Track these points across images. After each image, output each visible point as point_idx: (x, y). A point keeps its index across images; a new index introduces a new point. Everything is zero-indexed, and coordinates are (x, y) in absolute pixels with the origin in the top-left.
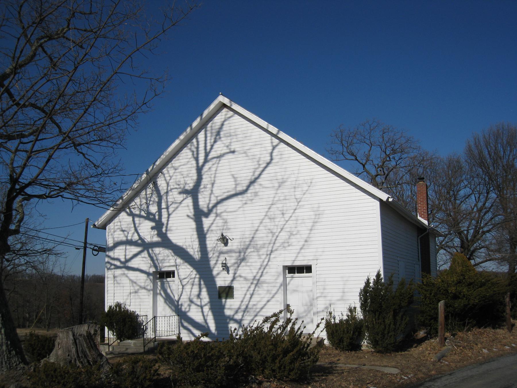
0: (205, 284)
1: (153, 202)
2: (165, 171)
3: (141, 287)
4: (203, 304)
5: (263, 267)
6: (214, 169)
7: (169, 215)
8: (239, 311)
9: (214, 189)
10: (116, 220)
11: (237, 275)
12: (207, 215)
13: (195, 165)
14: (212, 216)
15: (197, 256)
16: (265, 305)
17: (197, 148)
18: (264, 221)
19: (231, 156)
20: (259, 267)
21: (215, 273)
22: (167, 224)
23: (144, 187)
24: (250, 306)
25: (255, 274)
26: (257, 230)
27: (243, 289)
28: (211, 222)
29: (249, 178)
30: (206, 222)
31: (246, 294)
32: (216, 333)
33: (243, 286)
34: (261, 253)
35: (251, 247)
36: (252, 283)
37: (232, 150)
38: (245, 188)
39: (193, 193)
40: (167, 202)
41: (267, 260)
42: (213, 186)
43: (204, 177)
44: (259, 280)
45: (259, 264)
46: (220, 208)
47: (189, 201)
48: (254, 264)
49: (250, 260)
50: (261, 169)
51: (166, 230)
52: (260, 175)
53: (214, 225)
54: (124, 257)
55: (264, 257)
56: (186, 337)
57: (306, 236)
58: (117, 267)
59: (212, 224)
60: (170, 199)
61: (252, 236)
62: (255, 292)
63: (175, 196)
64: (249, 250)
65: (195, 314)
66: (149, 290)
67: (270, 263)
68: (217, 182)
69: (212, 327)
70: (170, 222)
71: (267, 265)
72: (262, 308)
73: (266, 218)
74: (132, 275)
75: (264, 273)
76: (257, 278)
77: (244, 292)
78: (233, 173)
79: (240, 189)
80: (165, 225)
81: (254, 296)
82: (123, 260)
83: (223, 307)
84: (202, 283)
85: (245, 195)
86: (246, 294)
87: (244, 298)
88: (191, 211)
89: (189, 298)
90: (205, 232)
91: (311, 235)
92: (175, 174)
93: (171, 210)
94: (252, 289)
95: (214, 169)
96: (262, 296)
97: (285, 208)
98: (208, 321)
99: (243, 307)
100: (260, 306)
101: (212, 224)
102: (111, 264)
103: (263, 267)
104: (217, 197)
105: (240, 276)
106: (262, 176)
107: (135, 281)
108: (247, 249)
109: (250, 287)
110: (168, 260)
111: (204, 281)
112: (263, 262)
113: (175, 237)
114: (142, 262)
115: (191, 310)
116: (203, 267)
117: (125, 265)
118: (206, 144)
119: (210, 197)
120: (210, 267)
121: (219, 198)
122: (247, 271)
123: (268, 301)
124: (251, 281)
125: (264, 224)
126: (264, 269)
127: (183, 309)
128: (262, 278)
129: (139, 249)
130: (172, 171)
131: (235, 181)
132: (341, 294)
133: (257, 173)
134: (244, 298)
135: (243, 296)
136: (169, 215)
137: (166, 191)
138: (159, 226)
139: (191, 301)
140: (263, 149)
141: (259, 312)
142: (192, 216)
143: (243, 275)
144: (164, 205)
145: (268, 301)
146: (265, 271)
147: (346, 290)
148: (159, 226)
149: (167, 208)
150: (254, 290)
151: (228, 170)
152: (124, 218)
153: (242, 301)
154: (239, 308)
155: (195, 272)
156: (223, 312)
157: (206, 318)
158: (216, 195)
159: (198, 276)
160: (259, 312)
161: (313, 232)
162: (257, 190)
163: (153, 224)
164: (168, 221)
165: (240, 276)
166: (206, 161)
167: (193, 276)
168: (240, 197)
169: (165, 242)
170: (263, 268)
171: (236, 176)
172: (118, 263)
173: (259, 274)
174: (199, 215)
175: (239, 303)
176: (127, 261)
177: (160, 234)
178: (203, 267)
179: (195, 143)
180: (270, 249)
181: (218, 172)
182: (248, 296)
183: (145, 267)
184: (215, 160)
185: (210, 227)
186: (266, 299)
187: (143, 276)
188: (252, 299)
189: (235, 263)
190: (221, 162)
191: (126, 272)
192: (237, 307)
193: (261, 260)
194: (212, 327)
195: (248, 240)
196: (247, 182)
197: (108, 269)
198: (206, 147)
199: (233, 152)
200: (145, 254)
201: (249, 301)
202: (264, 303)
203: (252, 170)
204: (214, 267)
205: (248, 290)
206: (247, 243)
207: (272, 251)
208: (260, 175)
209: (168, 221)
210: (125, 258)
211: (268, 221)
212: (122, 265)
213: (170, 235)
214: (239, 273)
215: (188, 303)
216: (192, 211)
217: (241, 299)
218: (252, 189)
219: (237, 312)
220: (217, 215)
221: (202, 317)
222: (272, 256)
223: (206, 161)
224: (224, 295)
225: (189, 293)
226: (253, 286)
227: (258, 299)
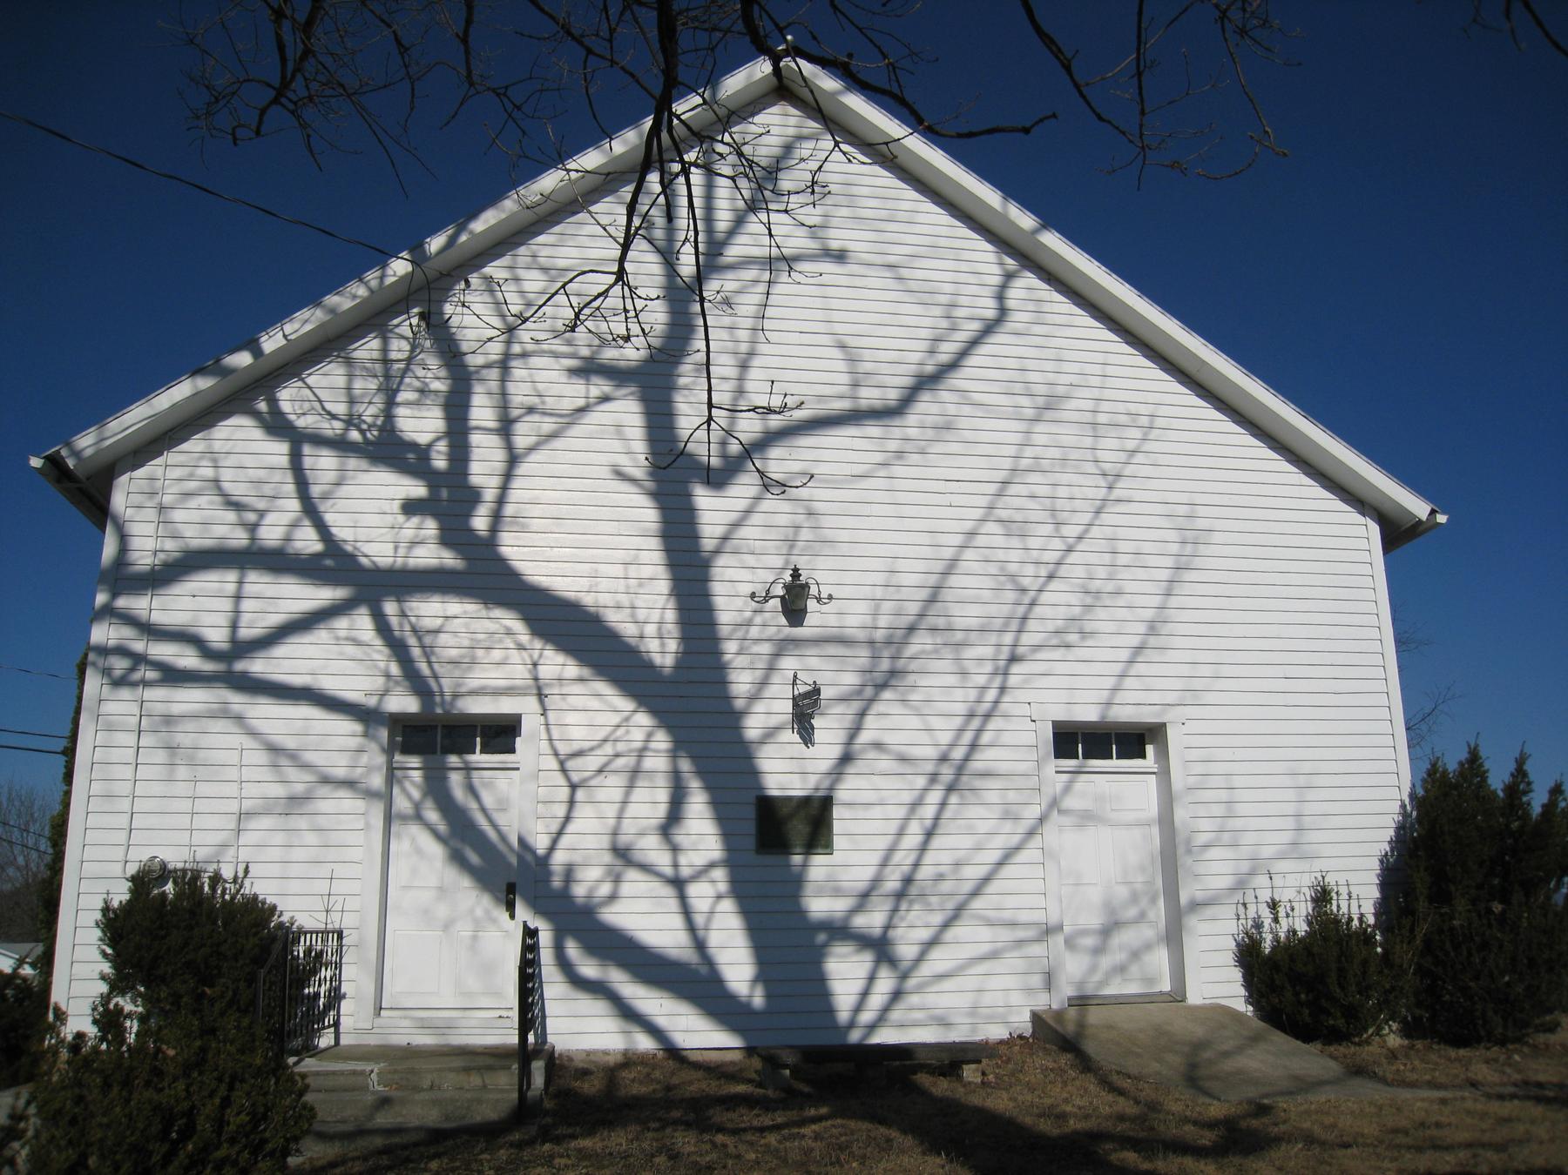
0: (701, 773)
1: (423, 391)
2: (495, 269)
3: (326, 780)
4: (691, 860)
5: (981, 716)
7: (513, 460)
10: (194, 445)
11: (865, 737)
12: (717, 479)
14: (744, 488)
15: (663, 650)
20: (961, 709)
21: (753, 726)
22: (504, 488)
23: (374, 319)
24: (925, 873)
25: (945, 738)
26: (955, 561)
28: (742, 504)
29: (916, 357)
30: (713, 510)
32: (758, 1001)
34: (970, 653)
36: (934, 777)
37: (834, 245)
38: (893, 395)
39: (654, 380)
40: (504, 394)
46: (779, 462)
47: (627, 412)
49: (924, 681)
50: (963, 336)
51: (497, 517)
52: (964, 353)
53: (756, 519)
54: (223, 620)
56: (581, 1028)
57: (1156, 601)
58: (173, 676)
59: (748, 512)
60: (520, 393)
61: (932, 580)
62: (948, 813)
63: (545, 380)
65: (645, 915)
66: (370, 794)
68: (763, 348)
69: (738, 968)
70: (516, 483)
74: (269, 715)
75: (986, 738)
76: (958, 753)
78: (839, 328)
79: (870, 396)
80: (490, 495)
82: (217, 636)
83: (795, 883)
84: (685, 765)
85: (897, 421)
87: (901, 833)
88: (635, 453)
89: (615, 833)
90: (708, 544)
91: (1173, 602)
93: (523, 435)
94: (935, 797)
96: (983, 827)
97: (1062, 492)
98: (714, 939)
100: (973, 873)
101: (748, 512)
102: (139, 659)
103: (981, 716)
106: (972, 360)
107: (290, 743)
108: (912, 629)
110: (485, 656)
111: (694, 758)
113: (531, 554)
114: (345, 658)
115: (626, 889)
116: (691, 700)
117: (231, 667)
120: (727, 698)
122: (913, 725)
124: (930, 767)
125: (980, 540)
126: (988, 716)
127: (579, 891)
129: (324, 595)
130: (534, 283)
131: (852, 360)
132: (1290, 823)
133: (947, 350)
134: (901, 833)
135: (893, 827)
136: (513, 460)
137: (496, 349)
138: (448, 499)
139: (623, 855)
140: (964, 267)
142: (639, 473)
143: (888, 738)
144: (482, 411)
146: (994, 724)
147: (1308, 809)
148: (448, 499)
149: (505, 427)
150: (943, 804)
151: (820, 315)
152: (241, 445)
153: (891, 850)
154: (876, 882)
155: (644, 719)
157: (701, 933)
159: (662, 741)
161: (1177, 589)
162: (952, 409)
163: (418, 490)
164: (508, 476)
167: (638, 735)
168: (873, 430)
169: (485, 575)
171: (850, 341)
172: (187, 659)
174: (673, 475)
175: (876, 858)
176: (242, 648)
177: (455, 533)
178: (691, 700)
180: (1008, 638)
181: (769, 312)
182: (915, 828)
183: (356, 685)
185: (736, 525)
187: (345, 729)
188: (936, 842)
191: (237, 701)
192: (868, 873)
194: (738, 968)
197: (119, 683)
199: (840, 256)
200: (362, 622)
204: (754, 698)
205: (916, 805)
208: (964, 353)
209: (508, 476)
210: (234, 626)
212: (209, 666)
213: (516, 549)
215: (607, 858)
216: (640, 447)
217: (884, 843)
218: (927, 407)
220: (767, 484)
221: (678, 921)
222: (1016, 668)
224: (798, 829)
225: (611, 811)
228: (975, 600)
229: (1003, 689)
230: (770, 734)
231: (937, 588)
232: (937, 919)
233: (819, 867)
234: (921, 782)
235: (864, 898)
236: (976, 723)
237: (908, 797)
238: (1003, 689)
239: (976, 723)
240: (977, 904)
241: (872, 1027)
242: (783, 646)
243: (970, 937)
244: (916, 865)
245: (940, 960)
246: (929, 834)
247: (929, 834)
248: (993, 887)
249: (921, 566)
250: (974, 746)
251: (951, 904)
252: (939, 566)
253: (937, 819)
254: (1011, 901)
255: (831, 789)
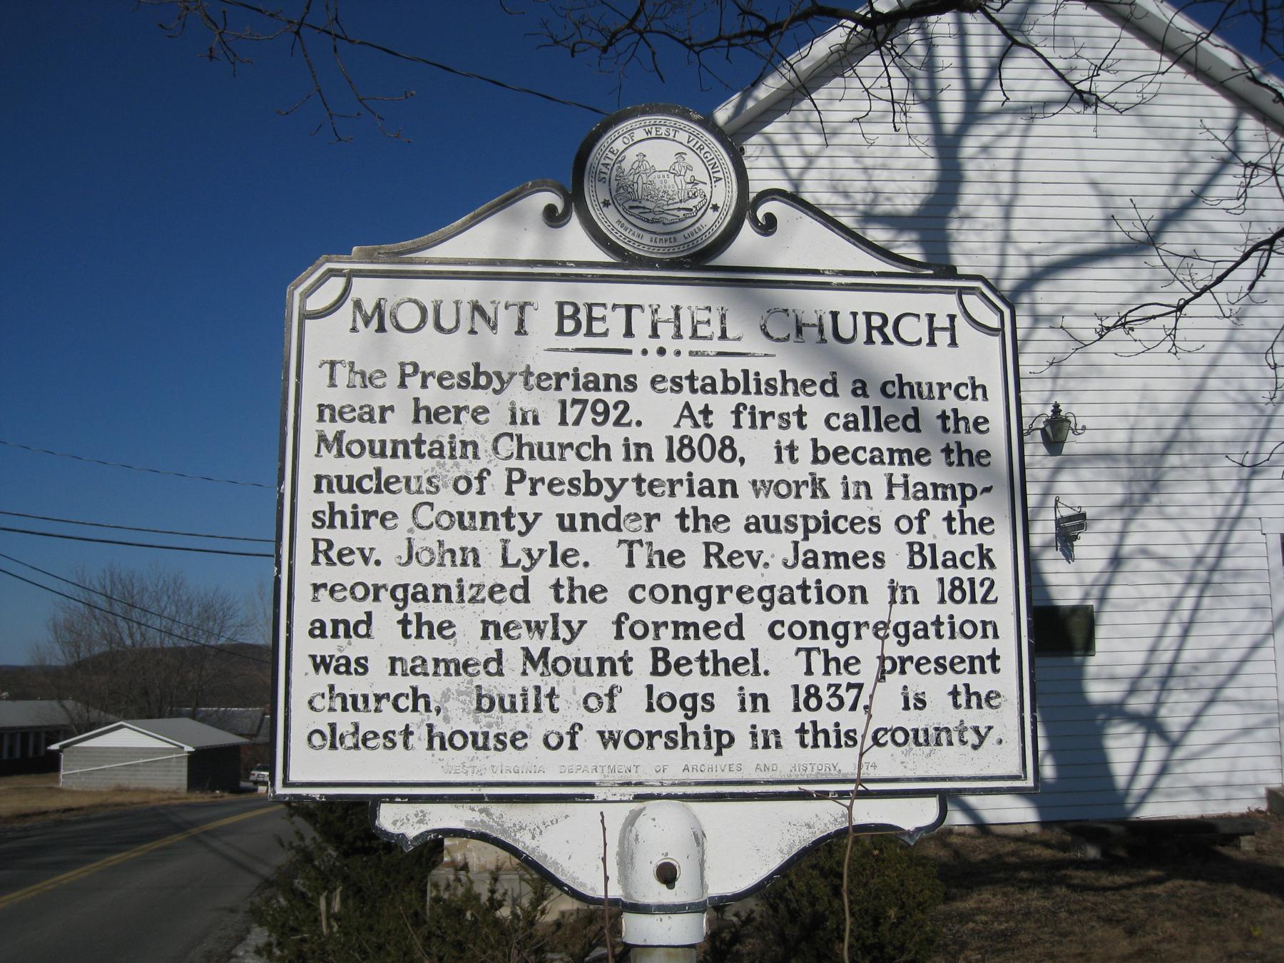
6: (1005, 151)
8: (1146, 683)
9: (1016, 224)
13: (927, 128)
16: (1243, 661)
17: (930, 65)
18: (1226, 359)
19: (1075, 116)
20: (1211, 525)
24: (1180, 668)
25: (1198, 549)
26: (1199, 390)
27: (1153, 605)
31: (1165, 624)
33: (1148, 591)
35: (1176, 447)
36: (1189, 583)
41: (1238, 500)
42: (1007, 217)
43: (971, 175)
44: (1212, 570)
45: (1208, 512)
48: (1194, 512)
50: (1198, 179)
55: (1228, 487)
61: (1180, 410)
62: (1201, 614)
64: (1173, 460)
67: (1249, 511)
71: (1238, 518)
72: (1233, 674)
73: (1233, 348)
75: (1230, 547)
76: (1210, 561)
77: (1160, 617)
81: (1195, 631)
86: (1165, 624)
87: (1160, 637)
92: (828, 152)
94: (1188, 603)
95: (1005, 151)
99: (1157, 671)
104: (1029, 255)
105: (1145, 552)
108: (1163, 454)
109: (1180, 597)
112: (1228, 505)
118: (964, 57)
119: (1003, 255)
121: (1038, 261)
123: (1255, 647)
125: (1221, 371)
126: (1231, 530)
128: (1228, 563)
134: (1160, 637)
135: (1155, 630)
141: (1219, 688)
145: (1255, 647)
146: (1236, 537)
150: (1196, 609)
153: (1153, 651)
156: (1081, 693)
158: (1026, 247)
160: (1219, 688)
165: (1145, 552)
166: (972, 114)
170: (1225, 527)
173: (1213, 552)
175: (1140, 658)
179: (920, 50)
182: (1174, 630)
184: (1007, 119)
186: (1245, 641)
188: (1191, 642)
189: (1121, 506)
190: (1036, 130)
192: (1134, 670)
193: (1220, 500)
195: (1171, 423)
196: (1151, 214)
198: (964, 68)
201: (1179, 650)
202: (1236, 654)
203: (1169, 179)
205: (1173, 609)
206: (1167, 434)
207: (1255, 469)
211: (1238, 359)
214: (1133, 540)
217: (1147, 643)
219: (1132, 691)
222: (1257, 485)
223: (972, 114)
226: (1193, 592)
227: (1219, 641)
228: (1221, 425)
229: (1245, 504)
230: (1046, 546)
231: (1186, 416)
232: (1195, 707)
233: (1094, 663)
234: (1176, 590)
235: (1132, 691)
236: (1221, 535)
237: (1167, 603)
238: (1245, 504)
239: (1221, 535)
240: (1228, 693)
241: (1142, 799)
242: (1058, 469)
243: (1224, 718)
244: (1174, 662)
245: (1197, 739)
246: (1185, 634)
247: (1185, 634)
248: (1242, 679)
249: (1170, 397)
250: (1221, 556)
251: (1205, 695)
252: (1185, 397)
253: (1191, 622)
254: (1256, 694)
255: (1102, 599)
